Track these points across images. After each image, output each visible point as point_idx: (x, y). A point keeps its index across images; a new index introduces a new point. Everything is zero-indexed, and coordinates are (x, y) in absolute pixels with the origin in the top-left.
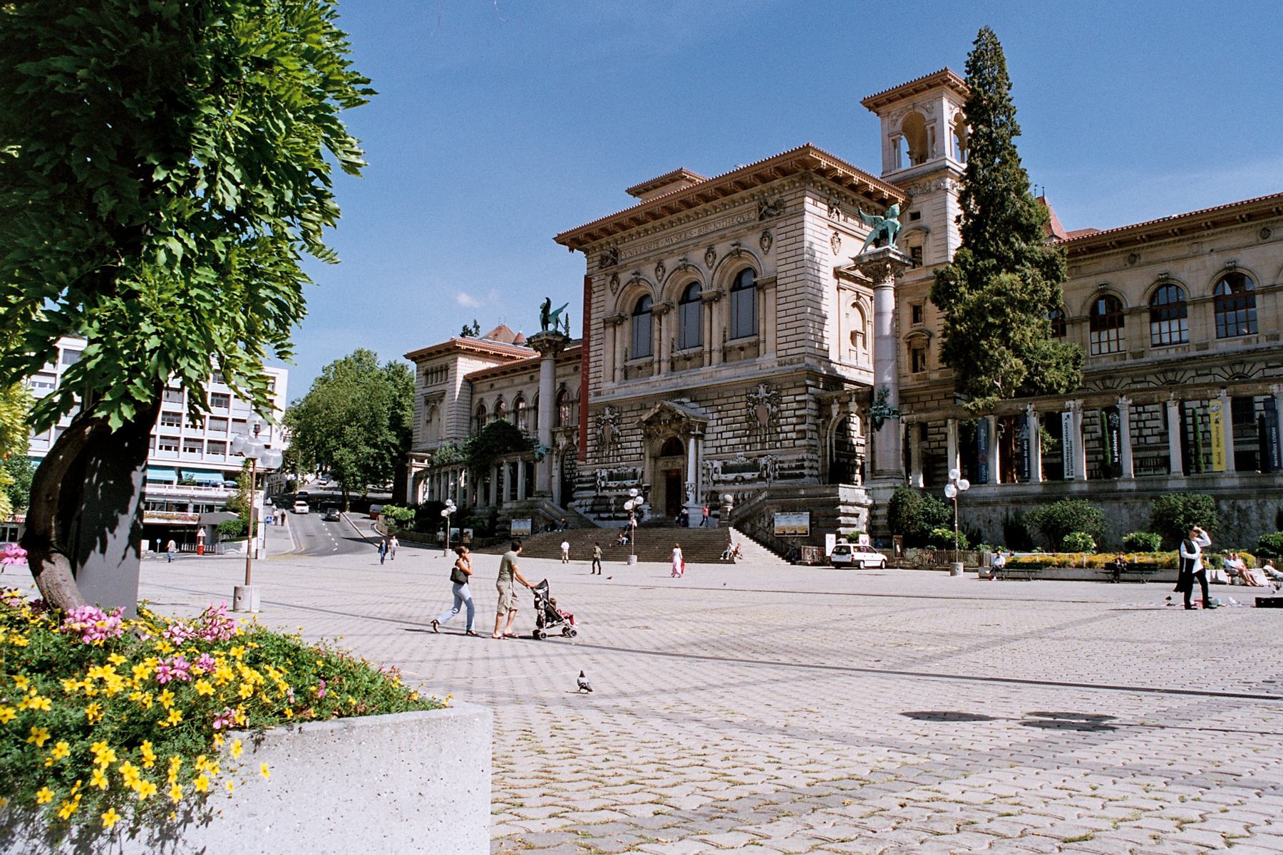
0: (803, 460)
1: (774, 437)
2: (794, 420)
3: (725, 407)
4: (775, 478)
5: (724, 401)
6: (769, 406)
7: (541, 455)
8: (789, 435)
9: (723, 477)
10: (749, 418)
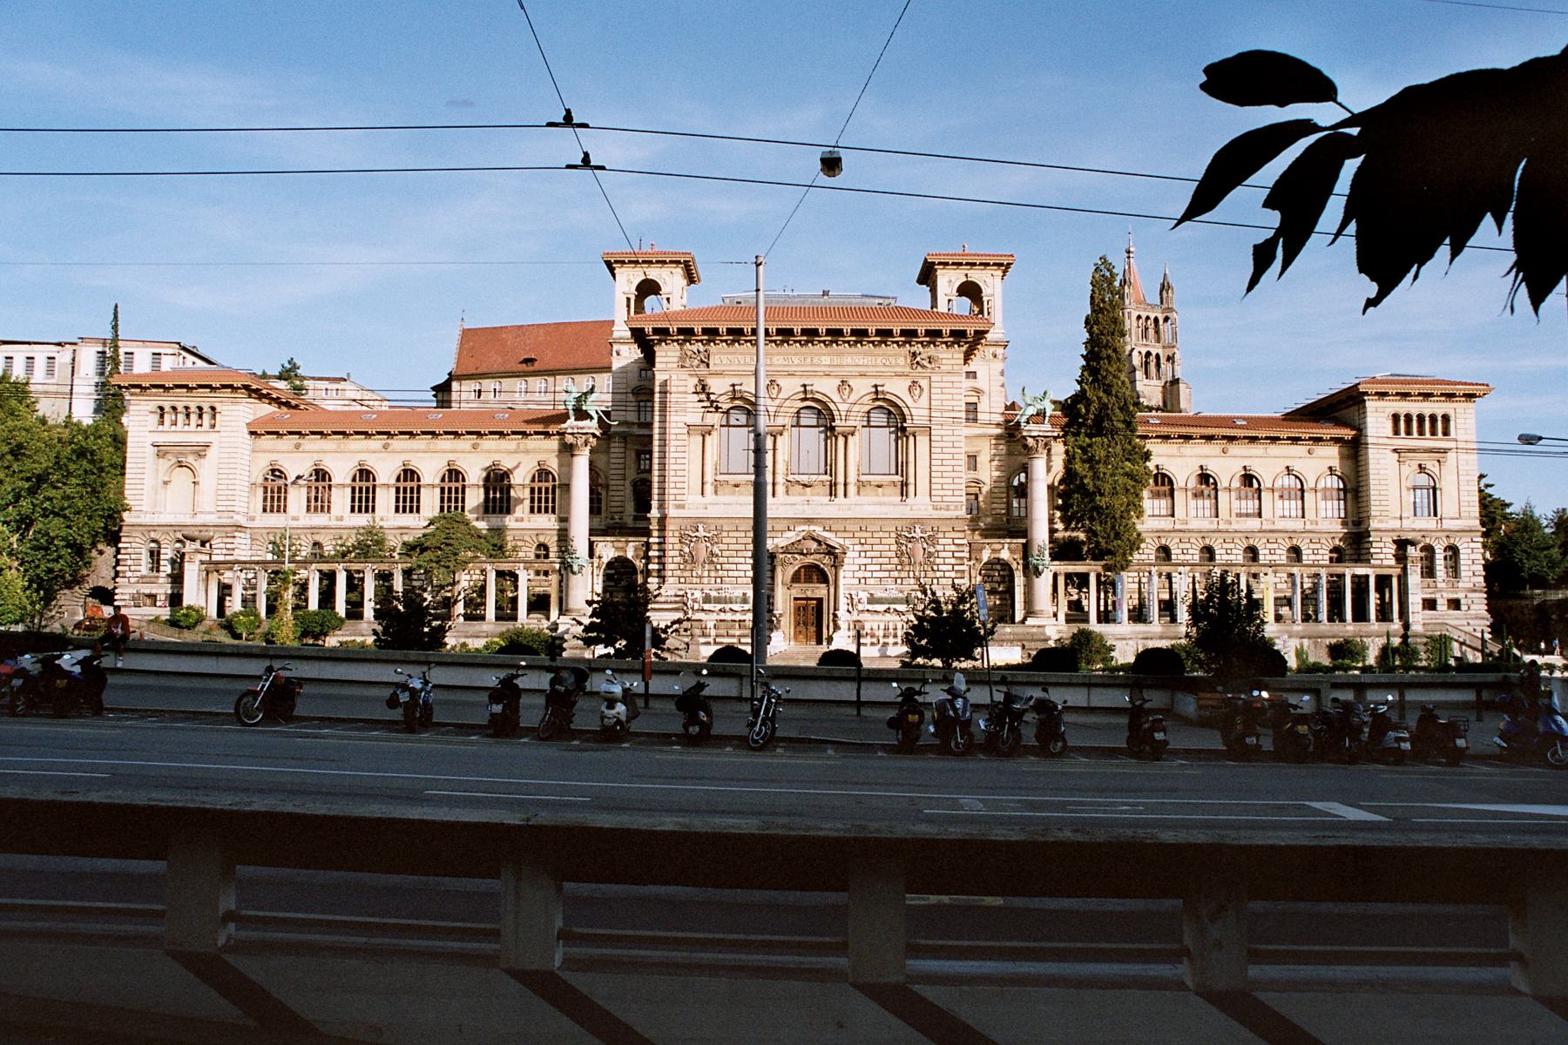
1: (930, 574)
2: (953, 561)
7: (581, 567)
9: (870, 607)
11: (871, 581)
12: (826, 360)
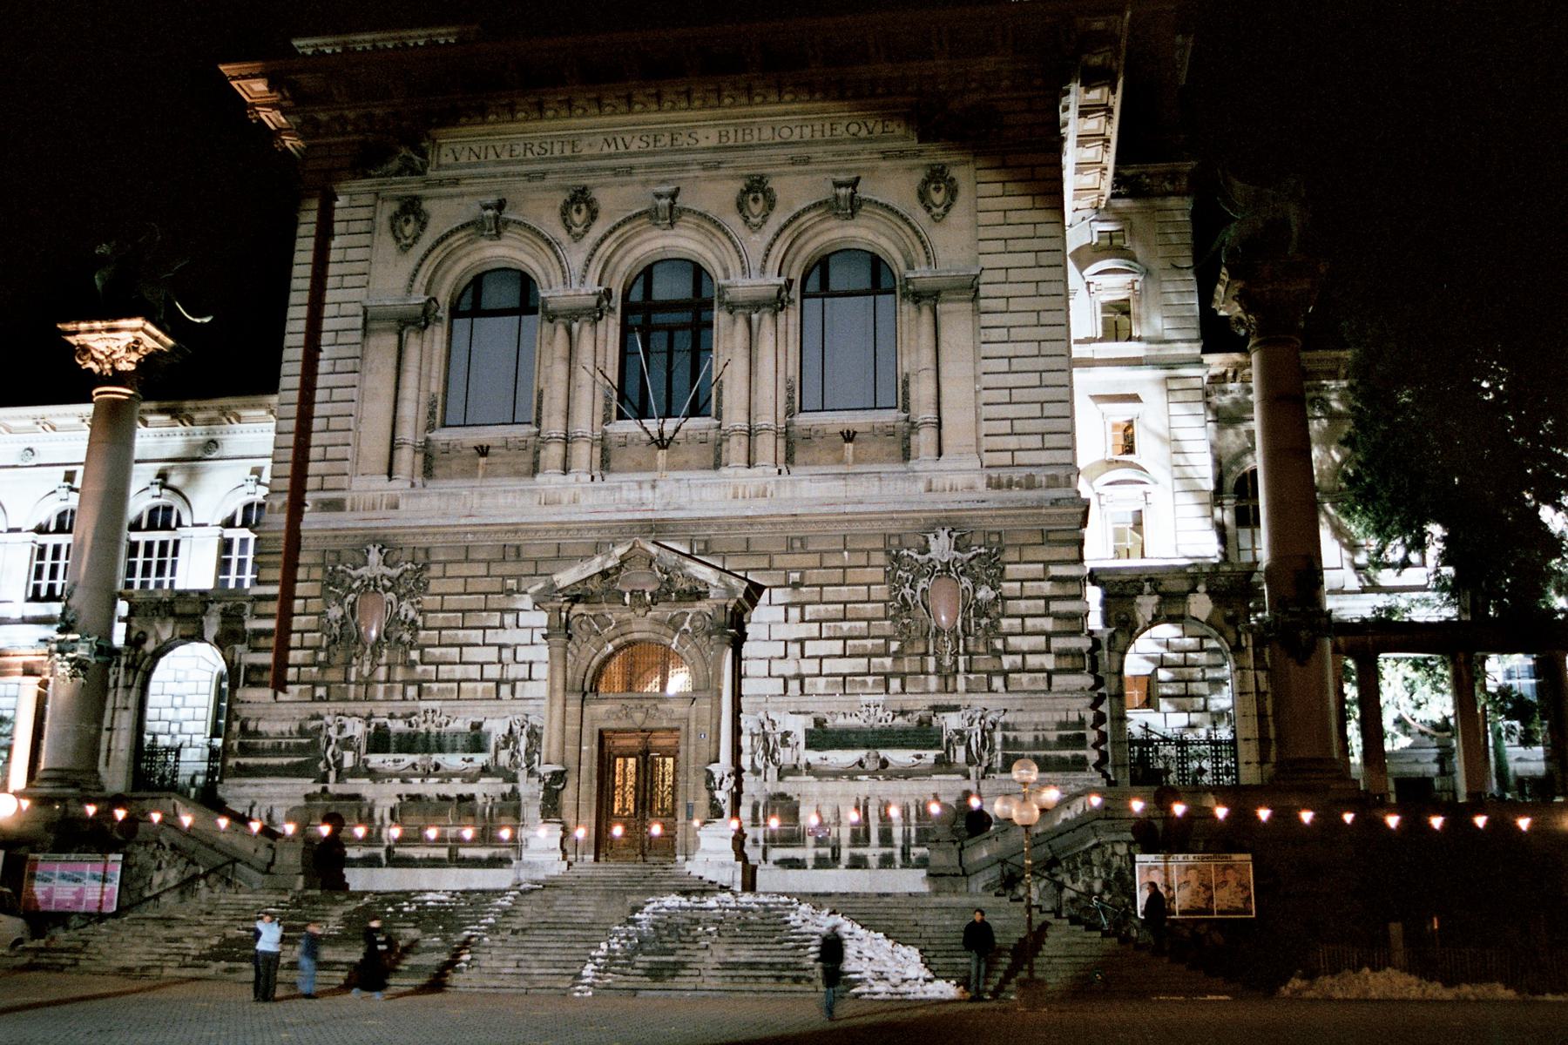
0: (1082, 723)
1: (984, 662)
2: (1048, 624)
3: (814, 576)
4: (989, 769)
5: (813, 560)
6: (966, 582)
8: (1033, 661)
11: (822, 681)
12: (708, 137)
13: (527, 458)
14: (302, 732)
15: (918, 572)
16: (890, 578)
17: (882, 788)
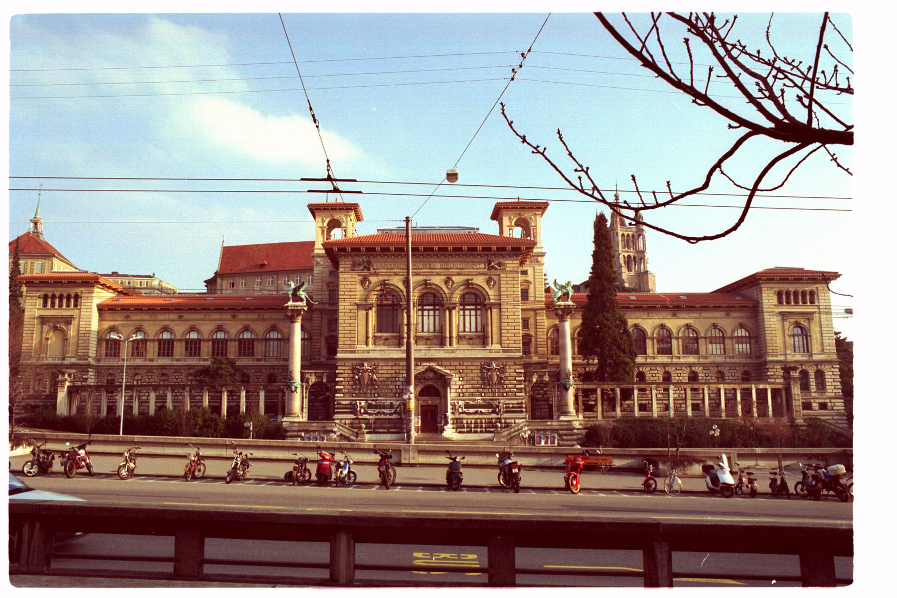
9: (466, 410)
10: (483, 378)
12: (438, 265)
13: (396, 341)
14: (351, 404)
15: (488, 370)
16: (482, 372)
17: (481, 416)
